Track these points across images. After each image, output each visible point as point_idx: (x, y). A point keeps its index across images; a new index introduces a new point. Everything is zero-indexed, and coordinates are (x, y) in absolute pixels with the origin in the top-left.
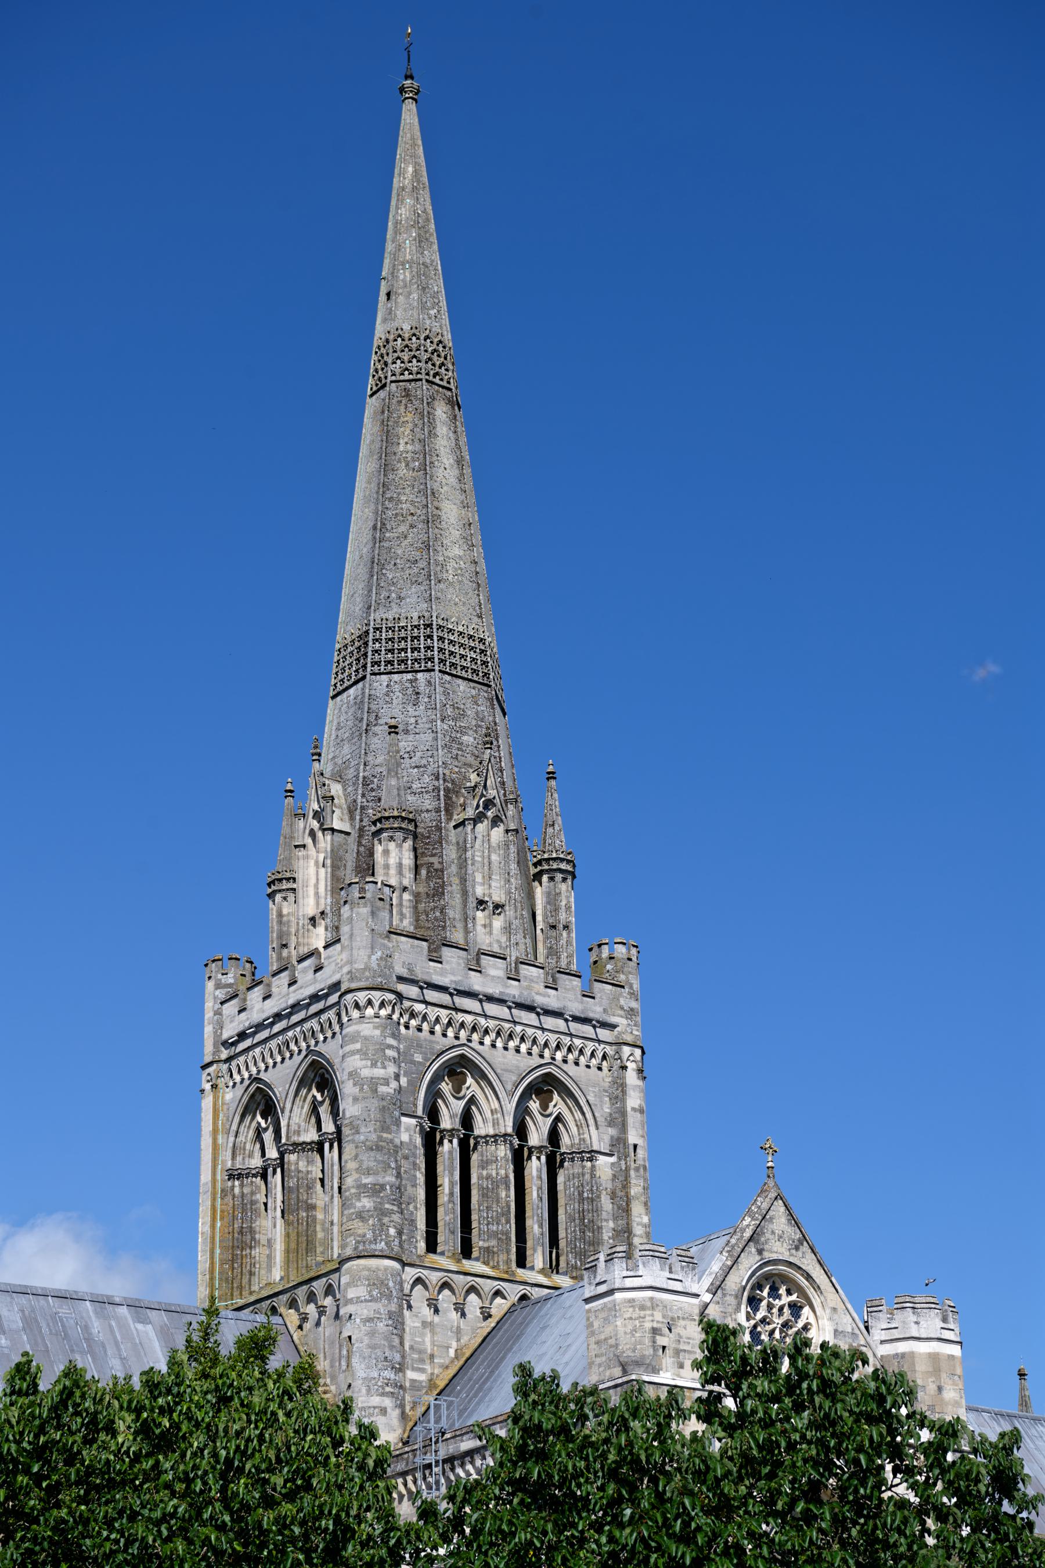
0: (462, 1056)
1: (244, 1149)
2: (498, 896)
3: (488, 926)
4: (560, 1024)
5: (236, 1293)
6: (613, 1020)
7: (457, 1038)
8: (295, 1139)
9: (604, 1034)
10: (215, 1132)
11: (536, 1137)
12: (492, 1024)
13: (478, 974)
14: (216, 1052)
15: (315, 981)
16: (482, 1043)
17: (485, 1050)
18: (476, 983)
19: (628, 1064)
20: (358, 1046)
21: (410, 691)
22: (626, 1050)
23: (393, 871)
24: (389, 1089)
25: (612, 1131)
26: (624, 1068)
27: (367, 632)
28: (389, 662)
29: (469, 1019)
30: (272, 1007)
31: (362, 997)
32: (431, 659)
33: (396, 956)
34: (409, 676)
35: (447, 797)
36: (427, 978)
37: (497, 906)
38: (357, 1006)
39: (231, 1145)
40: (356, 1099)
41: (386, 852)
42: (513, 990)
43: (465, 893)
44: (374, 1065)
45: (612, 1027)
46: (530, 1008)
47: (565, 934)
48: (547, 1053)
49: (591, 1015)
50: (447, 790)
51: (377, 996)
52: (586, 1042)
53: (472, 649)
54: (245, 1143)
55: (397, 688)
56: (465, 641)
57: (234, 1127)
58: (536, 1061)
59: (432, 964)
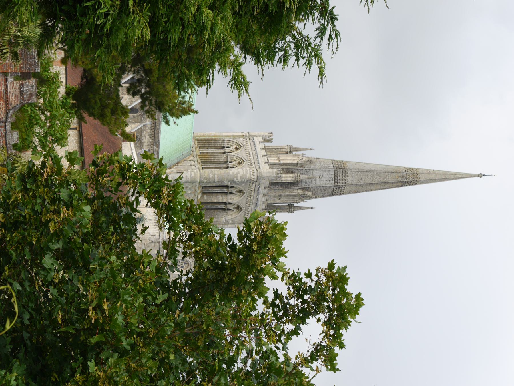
5: (198, 142)
8: (229, 156)
10: (233, 136)
11: (229, 207)
14: (251, 136)
15: (262, 162)
18: (260, 196)
21: (330, 179)
23: (286, 178)
24: (235, 179)
27: (345, 169)
28: (337, 174)
29: (252, 194)
30: (258, 150)
32: (337, 184)
33: (265, 181)
34: (333, 179)
35: (304, 188)
39: (230, 140)
41: (290, 177)
42: (260, 203)
44: (240, 177)
50: (306, 188)
53: (341, 192)
55: (331, 176)
56: (342, 190)
57: (234, 141)
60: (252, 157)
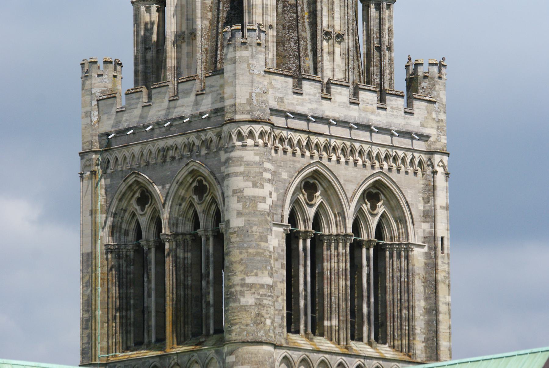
0: (316, 171)
1: (121, 228)
2: (338, 27)
3: (332, 53)
4: (385, 139)
6: (426, 131)
7: (312, 157)
9: (419, 145)
12: (339, 143)
13: (329, 102)
16: (329, 160)
17: (332, 165)
19: (437, 169)
20: (242, 169)
22: (437, 158)
25: (426, 226)
26: (435, 173)
29: (322, 140)
31: (245, 129)
36: (291, 108)
37: (338, 36)
38: (240, 136)
40: (239, 214)
43: (314, 24)
45: (424, 137)
46: (367, 127)
47: (387, 53)
48: (377, 165)
49: (409, 129)
51: (257, 129)
52: (406, 153)
54: (121, 223)
58: (371, 172)
59: (296, 96)
60: (180, 140)
